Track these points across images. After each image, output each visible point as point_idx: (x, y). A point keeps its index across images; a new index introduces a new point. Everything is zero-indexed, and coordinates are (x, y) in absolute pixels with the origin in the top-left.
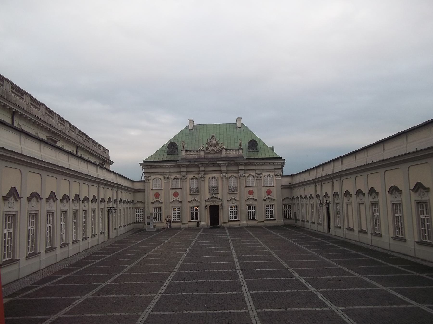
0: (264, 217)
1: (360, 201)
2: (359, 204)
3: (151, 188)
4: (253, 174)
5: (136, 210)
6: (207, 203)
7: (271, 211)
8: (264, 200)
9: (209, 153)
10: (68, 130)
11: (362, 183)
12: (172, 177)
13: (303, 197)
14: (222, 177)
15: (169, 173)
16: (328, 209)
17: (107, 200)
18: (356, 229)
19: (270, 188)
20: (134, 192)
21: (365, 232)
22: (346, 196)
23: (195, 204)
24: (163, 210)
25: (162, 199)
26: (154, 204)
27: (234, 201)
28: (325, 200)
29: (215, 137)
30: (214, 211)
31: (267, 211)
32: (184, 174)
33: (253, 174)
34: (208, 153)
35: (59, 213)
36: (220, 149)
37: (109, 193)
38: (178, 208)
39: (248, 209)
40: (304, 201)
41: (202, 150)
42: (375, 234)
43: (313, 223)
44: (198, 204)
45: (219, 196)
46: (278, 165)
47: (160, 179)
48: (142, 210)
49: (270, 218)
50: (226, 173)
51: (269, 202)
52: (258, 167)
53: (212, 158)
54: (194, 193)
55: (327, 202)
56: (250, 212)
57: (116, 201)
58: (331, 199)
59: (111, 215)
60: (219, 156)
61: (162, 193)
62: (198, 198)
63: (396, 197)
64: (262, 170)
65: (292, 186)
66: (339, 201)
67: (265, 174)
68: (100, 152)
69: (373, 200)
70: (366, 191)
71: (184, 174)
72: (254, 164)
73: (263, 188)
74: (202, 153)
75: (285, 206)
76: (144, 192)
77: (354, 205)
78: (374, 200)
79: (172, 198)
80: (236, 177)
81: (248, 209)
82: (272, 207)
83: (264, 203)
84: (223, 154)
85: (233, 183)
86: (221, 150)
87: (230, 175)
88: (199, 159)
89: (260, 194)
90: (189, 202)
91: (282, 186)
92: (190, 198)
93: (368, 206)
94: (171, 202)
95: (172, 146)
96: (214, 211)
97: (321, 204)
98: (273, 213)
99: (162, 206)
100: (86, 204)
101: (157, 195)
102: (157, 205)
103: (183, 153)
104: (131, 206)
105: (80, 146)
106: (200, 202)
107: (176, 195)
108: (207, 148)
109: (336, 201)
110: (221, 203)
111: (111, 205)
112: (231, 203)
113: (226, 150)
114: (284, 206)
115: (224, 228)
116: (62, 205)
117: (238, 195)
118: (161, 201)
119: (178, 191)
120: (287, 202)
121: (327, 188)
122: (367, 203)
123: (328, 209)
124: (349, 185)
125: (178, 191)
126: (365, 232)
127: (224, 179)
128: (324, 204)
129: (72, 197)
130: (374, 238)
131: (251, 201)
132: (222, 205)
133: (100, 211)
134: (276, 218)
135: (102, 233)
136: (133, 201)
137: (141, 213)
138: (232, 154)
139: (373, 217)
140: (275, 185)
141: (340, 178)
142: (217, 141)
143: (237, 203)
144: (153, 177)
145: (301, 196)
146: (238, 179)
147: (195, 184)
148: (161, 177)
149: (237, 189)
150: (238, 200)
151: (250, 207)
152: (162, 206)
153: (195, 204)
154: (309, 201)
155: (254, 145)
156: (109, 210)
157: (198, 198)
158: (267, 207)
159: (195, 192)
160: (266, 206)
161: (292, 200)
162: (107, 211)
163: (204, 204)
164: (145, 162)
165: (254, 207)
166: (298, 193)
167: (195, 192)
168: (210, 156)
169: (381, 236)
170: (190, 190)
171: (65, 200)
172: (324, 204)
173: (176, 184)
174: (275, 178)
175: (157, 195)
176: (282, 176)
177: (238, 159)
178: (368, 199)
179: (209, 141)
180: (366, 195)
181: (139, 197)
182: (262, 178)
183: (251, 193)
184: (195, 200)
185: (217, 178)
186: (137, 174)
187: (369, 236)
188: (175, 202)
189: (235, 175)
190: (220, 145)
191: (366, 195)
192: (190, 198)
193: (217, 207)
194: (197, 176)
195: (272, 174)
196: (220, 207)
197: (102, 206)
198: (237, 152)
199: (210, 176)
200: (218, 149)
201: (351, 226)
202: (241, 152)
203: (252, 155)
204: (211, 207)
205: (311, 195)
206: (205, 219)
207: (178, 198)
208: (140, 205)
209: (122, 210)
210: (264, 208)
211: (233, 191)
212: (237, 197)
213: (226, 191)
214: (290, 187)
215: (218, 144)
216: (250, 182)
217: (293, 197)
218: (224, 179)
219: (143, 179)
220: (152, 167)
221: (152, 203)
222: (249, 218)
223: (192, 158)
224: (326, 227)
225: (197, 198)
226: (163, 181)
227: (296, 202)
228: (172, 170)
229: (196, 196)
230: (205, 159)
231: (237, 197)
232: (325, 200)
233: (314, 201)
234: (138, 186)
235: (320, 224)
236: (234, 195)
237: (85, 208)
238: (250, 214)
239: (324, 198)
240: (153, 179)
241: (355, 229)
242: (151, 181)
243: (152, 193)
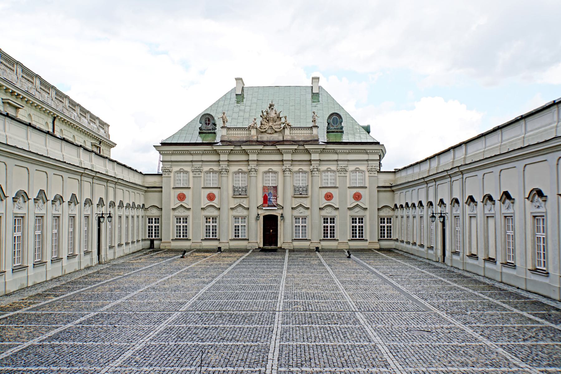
0: (349, 236)
1: (488, 212)
2: (488, 217)
3: (172, 186)
4: (334, 168)
5: (149, 219)
6: (260, 212)
7: (359, 227)
8: (350, 209)
9: (265, 132)
10: (39, 90)
11: (491, 183)
12: (206, 169)
13: (410, 205)
14: (284, 171)
15: (201, 163)
16: (443, 223)
17: (96, 201)
18: (481, 256)
19: (360, 191)
20: (146, 191)
21: (492, 260)
22: (469, 205)
23: (241, 212)
24: (190, 220)
25: (188, 203)
26: (177, 211)
27: (302, 210)
28: (439, 210)
29: (275, 107)
30: (270, 224)
31: (353, 227)
32: (224, 165)
34: (262, 132)
35: (10, 220)
36: (282, 126)
37: (100, 191)
39: (324, 223)
40: (411, 212)
41: (253, 128)
42: (506, 264)
43: (422, 246)
44: (245, 213)
46: (372, 153)
47: (187, 172)
48: (157, 220)
49: (358, 238)
50: (291, 165)
51: (358, 213)
52: (341, 157)
54: (240, 194)
55: (441, 213)
56: (327, 227)
57: (112, 204)
58: (448, 209)
59: (103, 225)
60: (281, 138)
63: (538, 207)
64: (348, 161)
65: (394, 189)
66: (458, 212)
67: (351, 168)
68: (94, 127)
69: (506, 211)
70: (496, 197)
71: (224, 165)
72: (335, 152)
73: (349, 190)
74: (253, 132)
75: (382, 220)
76: (162, 191)
77: (480, 218)
78: (508, 212)
80: (305, 172)
81: (324, 223)
82: (361, 220)
83: (350, 213)
85: (301, 181)
86: (284, 128)
87: (296, 168)
88: (249, 142)
89: (343, 199)
90: (232, 209)
91: (378, 187)
93: (499, 218)
94: (203, 209)
95: (207, 120)
96: (270, 224)
97: (433, 216)
98: (362, 230)
99: (189, 213)
100: (59, 207)
101: (182, 197)
102: (181, 213)
103: (224, 132)
104: (141, 212)
105: (58, 116)
106: (248, 209)
107: (211, 197)
108: (262, 124)
109: (454, 212)
110: (280, 212)
111: (103, 210)
112: (296, 213)
113: (291, 128)
114: (381, 219)
115: (284, 250)
116: (16, 206)
117: (309, 199)
118: (187, 207)
119: (215, 192)
120: (385, 213)
121: (443, 192)
122: (498, 216)
123: (443, 223)
124: (474, 186)
125: (215, 192)
126: (492, 260)
127: (288, 174)
128: (437, 216)
129: (33, 195)
130: (506, 270)
131: (329, 210)
132: (282, 216)
133: (83, 219)
134: (368, 238)
135: (87, 253)
136: (143, 205)
137: (157, 225)
138: (301, 135)
139: (505, 237)
140: (367, 185)
141: (461, 176)
142: (278, 113)
143: (307, 213)
144: (175, 169)
145: (407, 204)
146: (310, 173)
147: (241, 181)
149: (306, 190)
150: (308, 208)
151: (327, 219)
153: (241, 212)
154: (418, 211)
155: (336, 120)
156: (99, 218)
157: (245, 203)
158: (354, 220)
159: (240, 193)
160: (353, 219)
161: (393, 210)
162: (97, 218)
163: (254, 212)
164: (163, 144)
165: (333, 220)
166: (401, 198)
167: (240, 193)
168: (265, 137)
169: (514, 266)
170: (234, 191)
171: (21, 198)
172: (437, 216)
173: (212, 180)
174: (367, 174)
175: (182, 197)
176: (379, 172)
177: (310, 143)
178: (499, 209)
179: (265, 113)
180: (498, 203)
181: (153, 199)
182: (348, 175)
183: (329, 197)
184: (240, 205)
185: (276, 172)
186: (151, 162)
187: (480, 262)
188: (210, 208)
189: (305, 168)
190: (283, 120)
191: (498, 203)
192: (234, 203)
193: (277, 217)
194: (244, 169)
195: (363, 168)
196: (279, 218)
197: (87, 211)
198: (309, 131)
199: (266, 168)
200: (279, 127)
201: (474, 252)
202: (315, 131)
204: (265, 217)
205: (420, 203)
206: (257, 238)
207: (215, 203)
208: (154, 213)
209: (124, 219)
210: (349, 221)
211: (300, 193)
212: (306, 203)
213: (290, 192)
214: (391, 189)
215: (279, 118)
216: (329, 179)
217: (396, 205)
218: (288, 174)
219: (161, 172)
220: (174, 153)
221: (174, 209)
222: (324, 236)
223: (238, 139)
224: (440, 253)
225: (244, 203)
226: (191, 175)
227: (399, 212)
228: (205, 158)
229: (242, 200)
231: (306, 203)
232: (439, 210)
233: (424, 213)
234: (151, 182)
235: (431, 248)
236: (303, 200)
237: (57, 213)
238: (327, 230)
239: (439, 207)
240: (176, 172)
241: (479, 256)
242: (172, 175)
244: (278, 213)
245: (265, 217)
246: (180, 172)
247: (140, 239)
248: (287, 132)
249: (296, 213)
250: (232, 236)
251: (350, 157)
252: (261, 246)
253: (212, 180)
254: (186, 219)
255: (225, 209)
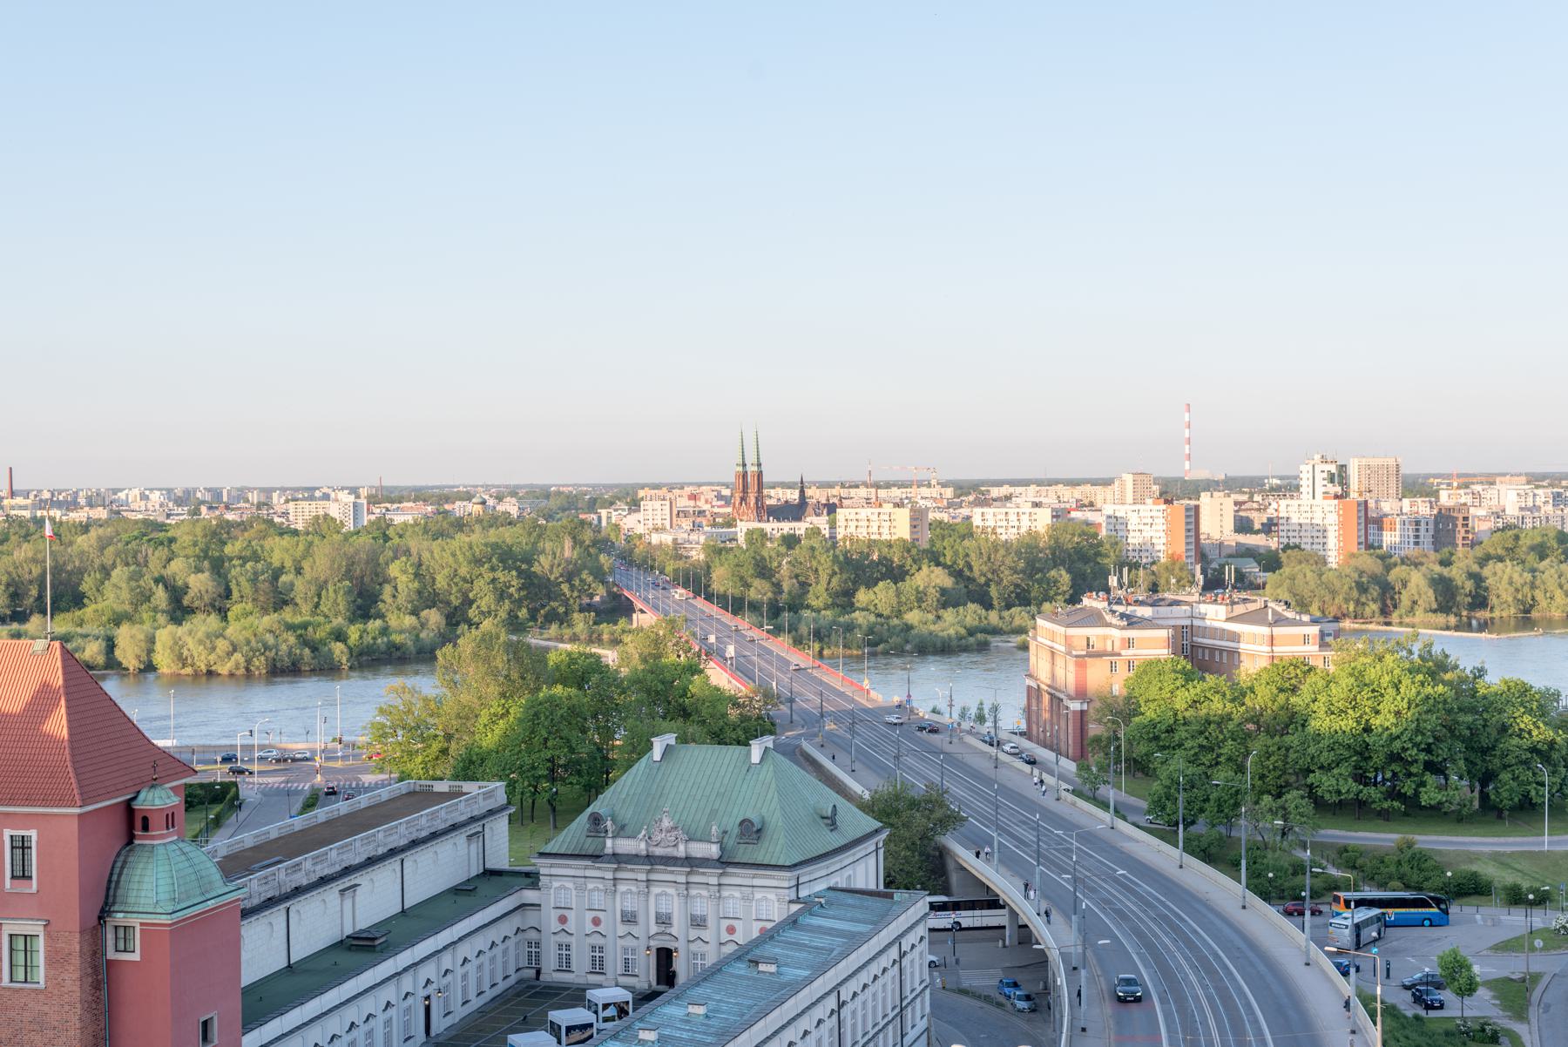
12: (590, 886)
25: (571, 926)
33: (737, 894)
38: (601, 949)
44: (634, 943)
45: (674, 931)
48: (538, 945)
53: (662, 857)
61: (571, 915)
62: (635, 930)
67: (758, 896)
74: (643, 846)
79: (590, 928)
84: (681, 851)
85: (699, 908)
92: (622, 929)
101: (563, 920)
102: (564, 939)
107: (596, 922)
125: (601, 915)
148: (570, 885)
152: (573, 940)
157: (635, 930)
159: (629, 918)
163: (643, 943)
168: (658, 851)
173: (598, 900)
175: (563, 920)
181: (531, 918)
194: (634, 889)
203: (744, 854)
204: (659, 950)
208: (533, 935)
211: (698, 922)
212: (705, 935)
218: (682, 900)
228: (589, 873)
230: (650, 859)
243: (555, 915)
244: (671, 945)
245: (659, 950)
246: (560, 888)
247: (511, 971)
248: (682, 847)
249: (694, 947)
250: (620, 970)
251: (757, 882)
252: (654, 983)
253: (598, 900)
254: (568, 947)
255: (610, 937)
